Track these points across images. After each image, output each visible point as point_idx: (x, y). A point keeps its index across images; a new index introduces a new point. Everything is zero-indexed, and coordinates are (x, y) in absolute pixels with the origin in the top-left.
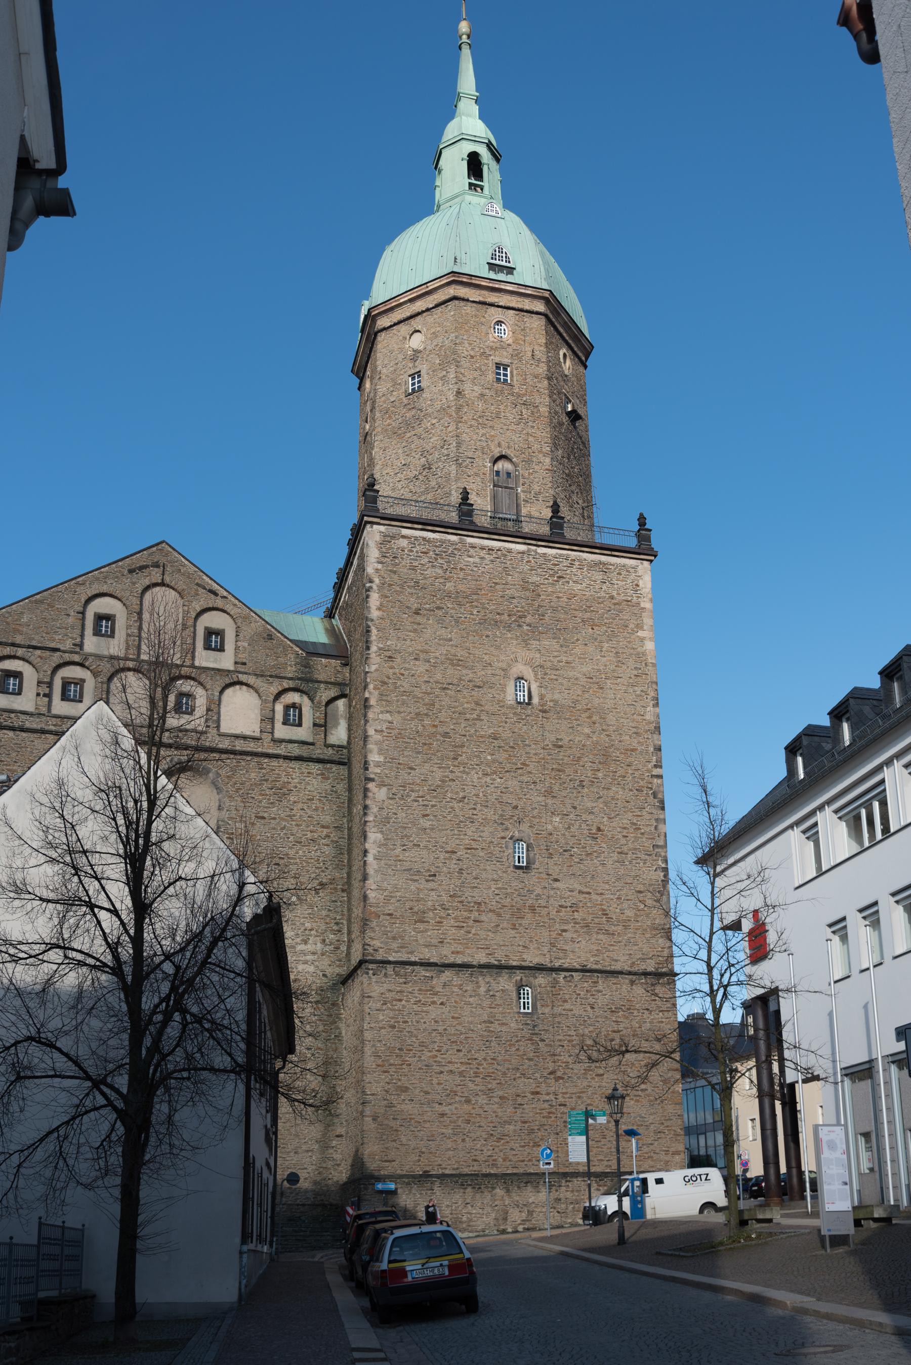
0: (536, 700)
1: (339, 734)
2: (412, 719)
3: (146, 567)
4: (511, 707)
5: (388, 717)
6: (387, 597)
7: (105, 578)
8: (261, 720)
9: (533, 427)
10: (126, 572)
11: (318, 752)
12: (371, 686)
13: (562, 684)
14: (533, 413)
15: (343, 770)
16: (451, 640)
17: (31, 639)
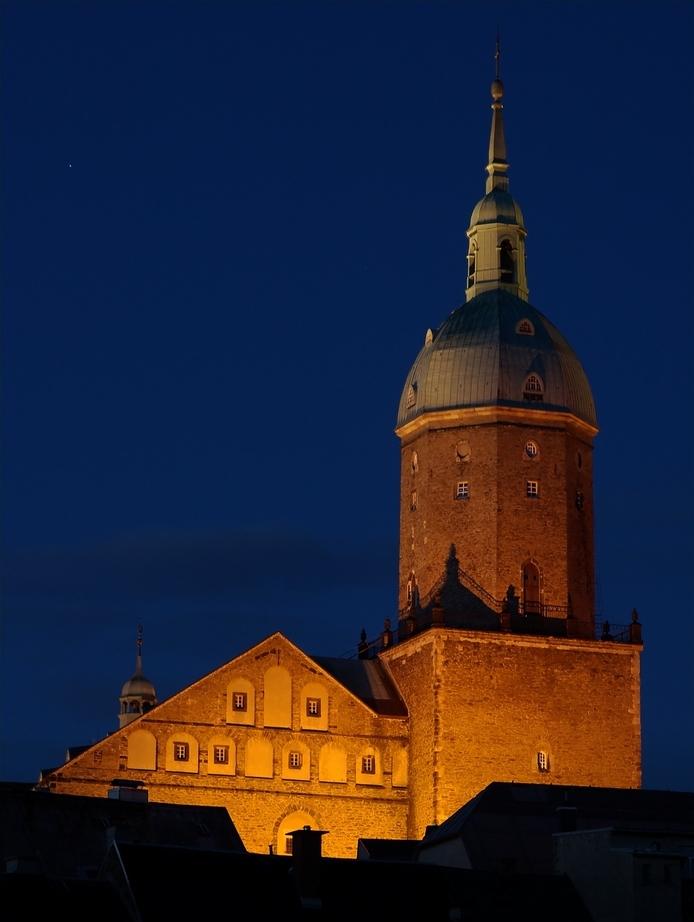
0: (552, 769)
1: (400, 777)
2: (467, 787)
3: (266, 654)
4: (535, 775)
5: (451, 786)
6: (450, 692)
7: (240, 665)
8: (348, 771)
9: (554, 535)
10: (254, 659)
11: (389, 794)
12: (439, 764)
13: (571, 755)
14: (554, 522)
15: (405, 809)
16: (494, 724)
17: (194, 718)
